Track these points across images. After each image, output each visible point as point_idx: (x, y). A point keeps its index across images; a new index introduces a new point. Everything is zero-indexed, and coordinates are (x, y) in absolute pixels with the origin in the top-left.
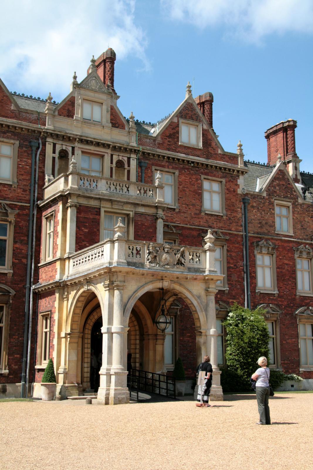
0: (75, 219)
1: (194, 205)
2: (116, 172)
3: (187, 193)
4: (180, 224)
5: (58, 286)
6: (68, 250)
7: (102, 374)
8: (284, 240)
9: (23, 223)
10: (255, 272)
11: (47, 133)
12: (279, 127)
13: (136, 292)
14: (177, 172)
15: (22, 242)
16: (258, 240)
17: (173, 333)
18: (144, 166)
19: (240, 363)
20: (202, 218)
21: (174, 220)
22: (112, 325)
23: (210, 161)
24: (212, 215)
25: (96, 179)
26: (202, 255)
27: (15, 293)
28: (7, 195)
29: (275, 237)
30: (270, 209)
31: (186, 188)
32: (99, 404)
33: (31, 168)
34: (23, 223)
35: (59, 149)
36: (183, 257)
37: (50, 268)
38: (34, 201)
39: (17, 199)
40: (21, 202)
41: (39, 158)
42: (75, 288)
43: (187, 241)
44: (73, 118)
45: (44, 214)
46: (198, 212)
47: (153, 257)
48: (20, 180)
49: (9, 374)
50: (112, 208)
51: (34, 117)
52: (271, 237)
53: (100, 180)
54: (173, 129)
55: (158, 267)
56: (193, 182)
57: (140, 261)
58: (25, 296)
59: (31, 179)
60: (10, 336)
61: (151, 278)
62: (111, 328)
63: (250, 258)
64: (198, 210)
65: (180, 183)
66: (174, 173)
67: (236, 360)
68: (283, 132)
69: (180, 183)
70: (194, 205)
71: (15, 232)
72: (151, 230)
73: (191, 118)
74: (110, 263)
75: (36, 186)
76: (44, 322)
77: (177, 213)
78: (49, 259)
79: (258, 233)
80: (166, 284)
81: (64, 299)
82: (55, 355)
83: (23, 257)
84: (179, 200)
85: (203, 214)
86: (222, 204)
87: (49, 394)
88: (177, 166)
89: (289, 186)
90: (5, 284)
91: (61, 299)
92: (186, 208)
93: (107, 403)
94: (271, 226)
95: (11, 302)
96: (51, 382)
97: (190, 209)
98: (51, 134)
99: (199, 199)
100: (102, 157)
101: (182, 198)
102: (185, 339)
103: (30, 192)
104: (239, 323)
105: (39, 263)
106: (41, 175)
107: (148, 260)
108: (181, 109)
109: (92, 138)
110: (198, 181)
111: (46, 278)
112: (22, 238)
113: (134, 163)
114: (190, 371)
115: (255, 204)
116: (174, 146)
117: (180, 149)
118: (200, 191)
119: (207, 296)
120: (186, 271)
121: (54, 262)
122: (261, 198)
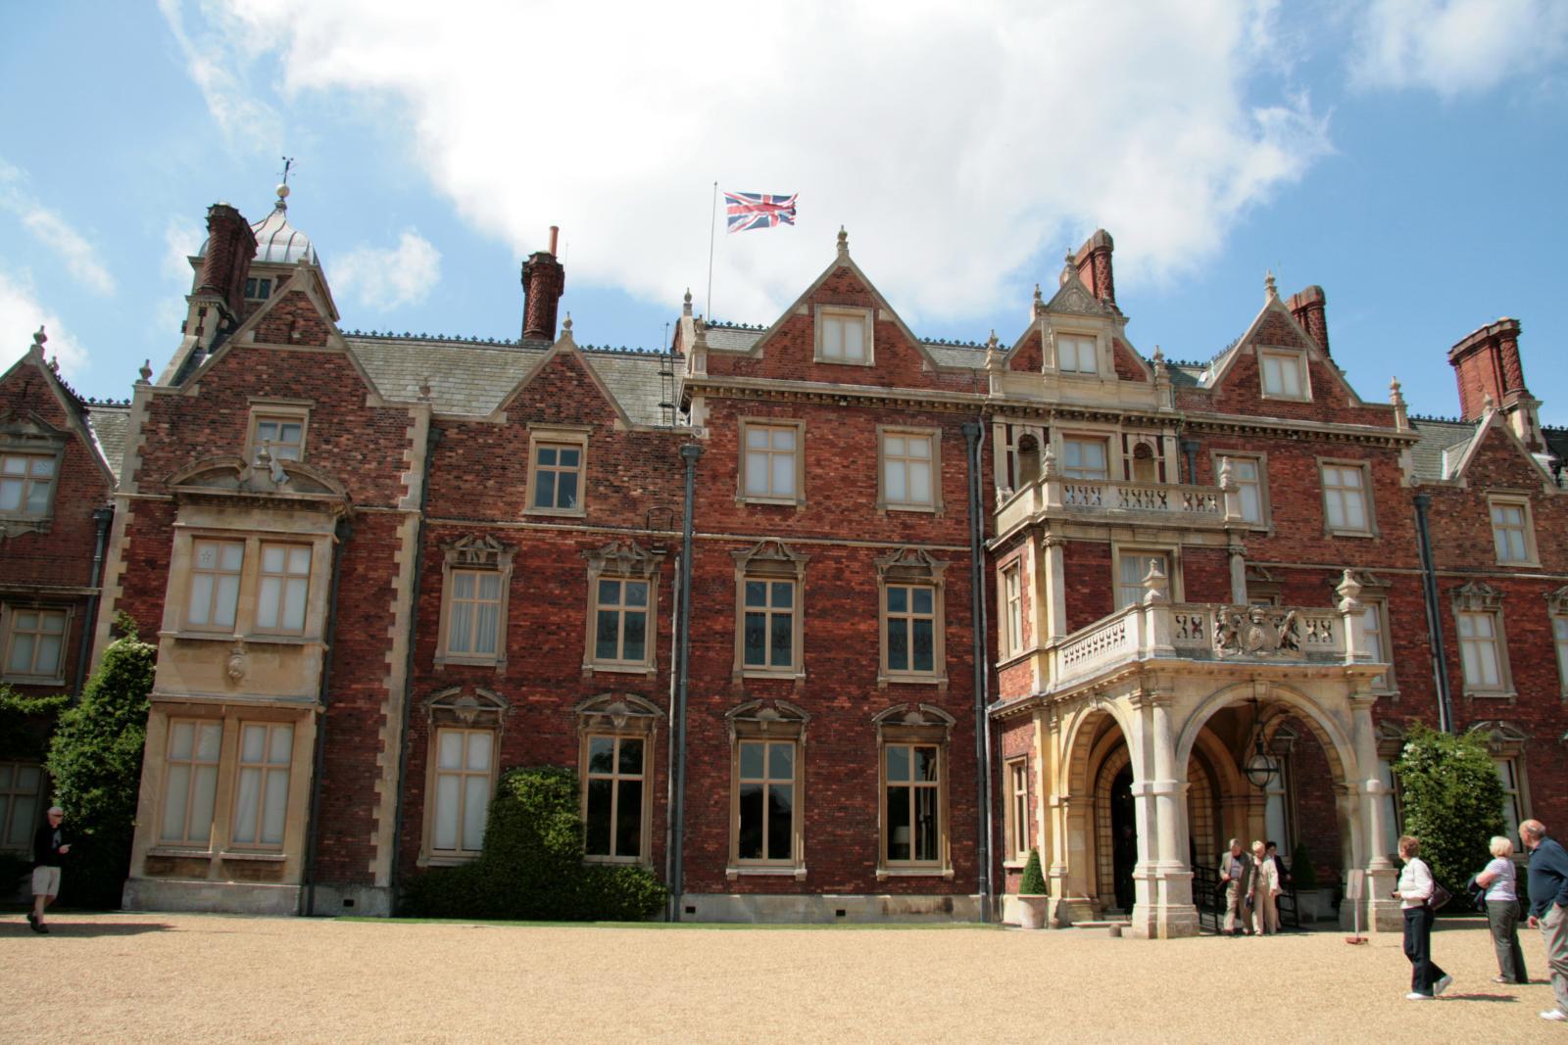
0: (1062, 571)
1: (1306, 521)
2: (1136, 470)
5: (1038, 705)
6: (1051, 633)
7: (1139, 879)
8: (1520, 579)
9: (960, 586)
10: (1457, 654)
11: (993, 406)
12: (1479, 338)
13: (1198, 708)
14: (1264, 456)
15: (960, 621)
16: (1457, 583)
17: (1283, 791)
19: (1440, 851)
20: (1327, 546)
21: (1267, 556)
22: (1154, 779)
23: (1332, 425)
24: (1348, 538)
25: (1097, 487)
26: (1336, 624)
27: (955, 721)
29: (1499, 575)
30: (1479, 514)
31: (1288, 486)
32: (1137, 936)
33: (968, 477)
34: (960, 586)
36: (1293, 632)
37: (1020, 669)
38: (978, 541)
39: (946, 540)
40: (954, 545)
42: (1072, 707)
44: (1040, 371)
45: (999, 564)
47: (1228, 635)
48: (949, 503)
49: (956, 877)
50: (1135, 542)
51: (967, 378)
52: (1488, 574)
53: (1104, 487)
54: (1246, 369)
55: (1242, 655)
57: (1202, 646)
58: (973, 727)
59: (969, 498)
60: (953, 805)
61: (1226, 680)
62: (1152, 785)
63: (1443, 623)
65: (1272, 478)
66: (1258, 459)
67: (1429, 845)
68: (1491, 347)
70: (1306, 521)
71: (947, 605)
73: (1283, 342)
74: (1141, 654)
75: (981, 511)
76: (1016, 776)
77: (1271, 541)
78: (1017, 653)
79: (1456, 569)
80: (1261, 690)
81: (1050, 729)
82: (1040, 840)
83: (967, 652)
84: (1273, 512)
85: (1328, 538)
86: (1369, 514)
87: (1034, 916)
89: (1517, 460)
90: (936, 705)
91: (1046, 731)
92: (1290, 528)
93: (1153, 935)
94: (1485, 551)
95: (949, 739)
96: (1036, 893)
98: (1001, 408)
100: (1106, 440)
103: (969, 524)
104: (1430, 765)
105: (997, 661)
107: (1219, 642)
111: (1012, 691)
112: (961, 615)
113: (1171, 447)
115: (1442, 507)
116: (1251, 402)
117: (1265, 409)
119: (1352, 709)
121: (1027, 657)
122: (1456, 493)
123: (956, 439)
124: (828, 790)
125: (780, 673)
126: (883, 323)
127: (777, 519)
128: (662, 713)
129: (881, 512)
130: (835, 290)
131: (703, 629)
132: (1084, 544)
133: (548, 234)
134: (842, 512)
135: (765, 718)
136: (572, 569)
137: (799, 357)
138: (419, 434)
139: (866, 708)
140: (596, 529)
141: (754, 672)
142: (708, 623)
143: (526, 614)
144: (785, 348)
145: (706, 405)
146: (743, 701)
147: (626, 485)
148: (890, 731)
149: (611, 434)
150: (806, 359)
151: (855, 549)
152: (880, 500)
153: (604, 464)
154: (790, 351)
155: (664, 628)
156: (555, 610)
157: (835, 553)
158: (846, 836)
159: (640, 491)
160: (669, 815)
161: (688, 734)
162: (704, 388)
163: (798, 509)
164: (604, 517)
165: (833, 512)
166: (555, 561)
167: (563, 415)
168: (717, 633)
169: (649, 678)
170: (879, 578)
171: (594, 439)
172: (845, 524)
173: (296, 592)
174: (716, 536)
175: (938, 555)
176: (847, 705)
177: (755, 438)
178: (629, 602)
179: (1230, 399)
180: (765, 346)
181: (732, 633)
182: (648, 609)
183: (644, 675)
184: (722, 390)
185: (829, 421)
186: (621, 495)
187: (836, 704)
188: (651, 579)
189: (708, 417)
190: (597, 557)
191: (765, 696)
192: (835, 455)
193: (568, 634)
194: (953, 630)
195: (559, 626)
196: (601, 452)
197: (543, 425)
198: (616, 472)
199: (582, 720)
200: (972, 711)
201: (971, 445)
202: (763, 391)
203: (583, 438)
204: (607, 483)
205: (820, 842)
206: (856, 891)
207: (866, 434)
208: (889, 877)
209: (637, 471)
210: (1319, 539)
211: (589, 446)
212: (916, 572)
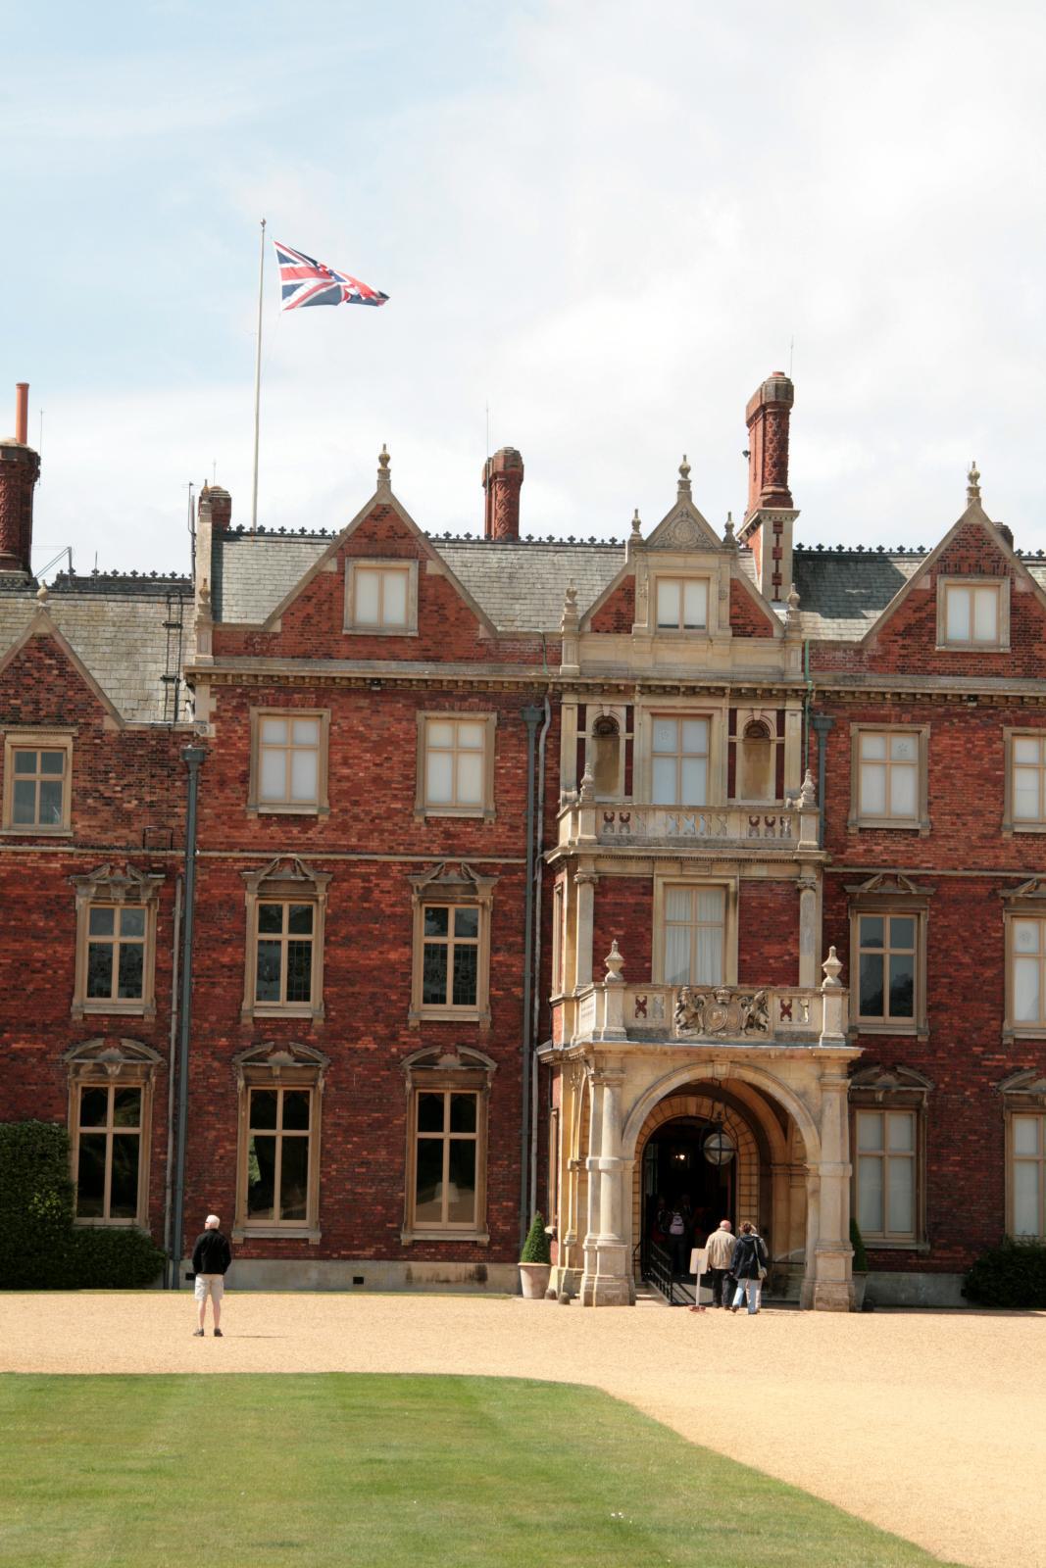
1: (978, 813)
2: (748, 752)
3: (958, 783)
4: (933, 868)
13: (652, 1088)
14: (926, 730)
15: (510, 947)
17: (913, 1153)
18: (824, 730)
20: (1004, 846)
21: (916, 861)
27: (496, 1065)
28: (473, 843)
31: (956, 768)
33: (527, 772)
35: (594, 719)
36: (763, 1012)
38: (535, 850)
39: (497, 850)
40: (506, 857)
41: (545, 745)
43: (954, 914)
46: (992, 832)
47: (689, 1015)
48: (503, 805)
49: (492, 1242)
50: (682, 876)
51: (533, 646)
54: (918, 609)
56: (978, 749)
57: (661, 1026)
60: (491, 1160)
61: (687, 1060)
62: (597, 1161)
64: (993, 826)
65: (934, 758)
66: (919, 732)
69: (936, 758)
70: (978, 813)
71: (495, 928)
72: (786, 918)
74: (596, 1035)
77: (924, 841)
83: (515, 984)
84: (930, 804)
85: (1006, 835)
88: (925, 713)
92: (953, 824)
93: (588, 1304)
95: (490, 1085)
96: (536, 1261)
97: (964, 824)
99: (993, 796)
100: (710, 717)
101: (942, 798)
102: (945, 1169)
103: (526, 831)
106: (551, 784)
107: (679, 1022)
108: (941, 550)
109: (675, 680)
110: (994, 746)
112: (511, 939)
113: (794, 724)
114: (959, 1252)
116: (919, 656)
118: (998, 773)
119: (822, 1091)
120: (769, 1040)
123: (515, 726)
124: (349, 1143)
125: (298, 1010)
126: (431, 578)
127: (295, 831)
128: (161, 1059)
129: (419, 820)
130: (371, 537)
131: (208, 962)
132: (622, 880)
133: (15, 394)
134: (372, 821)
135: (277, 1063)
136: (59, 897)
137: (325, 627)
139: (394, 1050)
140: (84, 851)
141: (268, 1010)
142: (214, 956)
143: (6, 950)
144: (309, 616)
145: (212, 694)
146: (254, 1044)
147: (119, 795)
148: (420, 1076)
149: (100, 734)
150: (332, 630)
151: (387, 864)
152: (418, 805)
153: (93, 772)
154: (313, 621)
155: (165, 962)
156: (40, 945)
157: (363, 870)
158: (367, 1194)
159: (135, 802)
160: (168, 1172)
161: (190, 1082)
162: (210, 675)
163: (320, 818)
164: (94, 834)
165: (362, 821)
166: (38, 888)
167: (42, 713)
168: (223, 966)
169: (147, 1019)
170: (414, 898)
171: (80, 741)
172: (376, 834)
174: (224, 854)
175: (484, 871)
176: (372, 1046)
177: (272, 729)
178: (124, 932)
179: (888, 653)
180: (284, 616)
181: (243, 966)
182: (146, 939)
183: (142, 1017)
184: (230, 678)
185: (359, 709)
186: (113, 808)
187: (360, 1045)
188: (149, 905)
189: (214, 709)
190: (87, 883)
191: (279, 1037)
192: (368, 752)
193: (55, 972)
194: (500, 958)
195: (44, 964)
196: (88, 757)
197: (19, 728)
198: (106, 780)
199: (71, 1069)
200: (518, 1052)
201: (532, 735)
202: (278, 677)
203: (67, 741)
204: (97, 794)
205: (338, 1202)
206: (378, 1257)
207: (404, 723)
208: (414, 1241)
209: (130, 779)
210: (993, 837)
211: (75, 750)
212: (458, 890)
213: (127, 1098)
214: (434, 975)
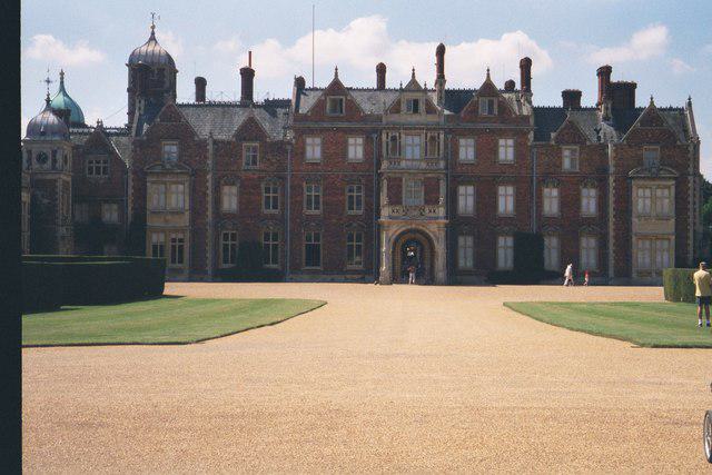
113: (442, 136)
138: (210, 147)
173: (181, 197)
177: (309, 140)
213: (275, 235)
214: (351, 203)
